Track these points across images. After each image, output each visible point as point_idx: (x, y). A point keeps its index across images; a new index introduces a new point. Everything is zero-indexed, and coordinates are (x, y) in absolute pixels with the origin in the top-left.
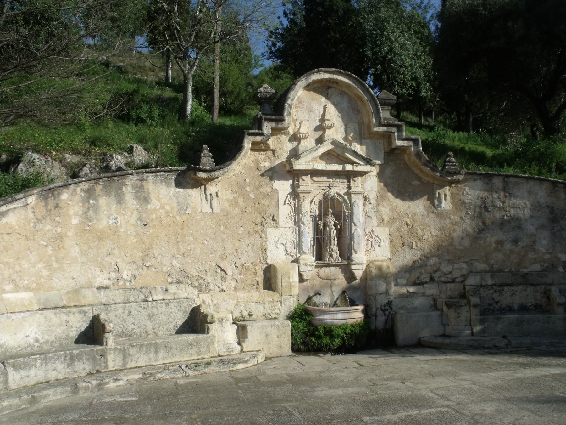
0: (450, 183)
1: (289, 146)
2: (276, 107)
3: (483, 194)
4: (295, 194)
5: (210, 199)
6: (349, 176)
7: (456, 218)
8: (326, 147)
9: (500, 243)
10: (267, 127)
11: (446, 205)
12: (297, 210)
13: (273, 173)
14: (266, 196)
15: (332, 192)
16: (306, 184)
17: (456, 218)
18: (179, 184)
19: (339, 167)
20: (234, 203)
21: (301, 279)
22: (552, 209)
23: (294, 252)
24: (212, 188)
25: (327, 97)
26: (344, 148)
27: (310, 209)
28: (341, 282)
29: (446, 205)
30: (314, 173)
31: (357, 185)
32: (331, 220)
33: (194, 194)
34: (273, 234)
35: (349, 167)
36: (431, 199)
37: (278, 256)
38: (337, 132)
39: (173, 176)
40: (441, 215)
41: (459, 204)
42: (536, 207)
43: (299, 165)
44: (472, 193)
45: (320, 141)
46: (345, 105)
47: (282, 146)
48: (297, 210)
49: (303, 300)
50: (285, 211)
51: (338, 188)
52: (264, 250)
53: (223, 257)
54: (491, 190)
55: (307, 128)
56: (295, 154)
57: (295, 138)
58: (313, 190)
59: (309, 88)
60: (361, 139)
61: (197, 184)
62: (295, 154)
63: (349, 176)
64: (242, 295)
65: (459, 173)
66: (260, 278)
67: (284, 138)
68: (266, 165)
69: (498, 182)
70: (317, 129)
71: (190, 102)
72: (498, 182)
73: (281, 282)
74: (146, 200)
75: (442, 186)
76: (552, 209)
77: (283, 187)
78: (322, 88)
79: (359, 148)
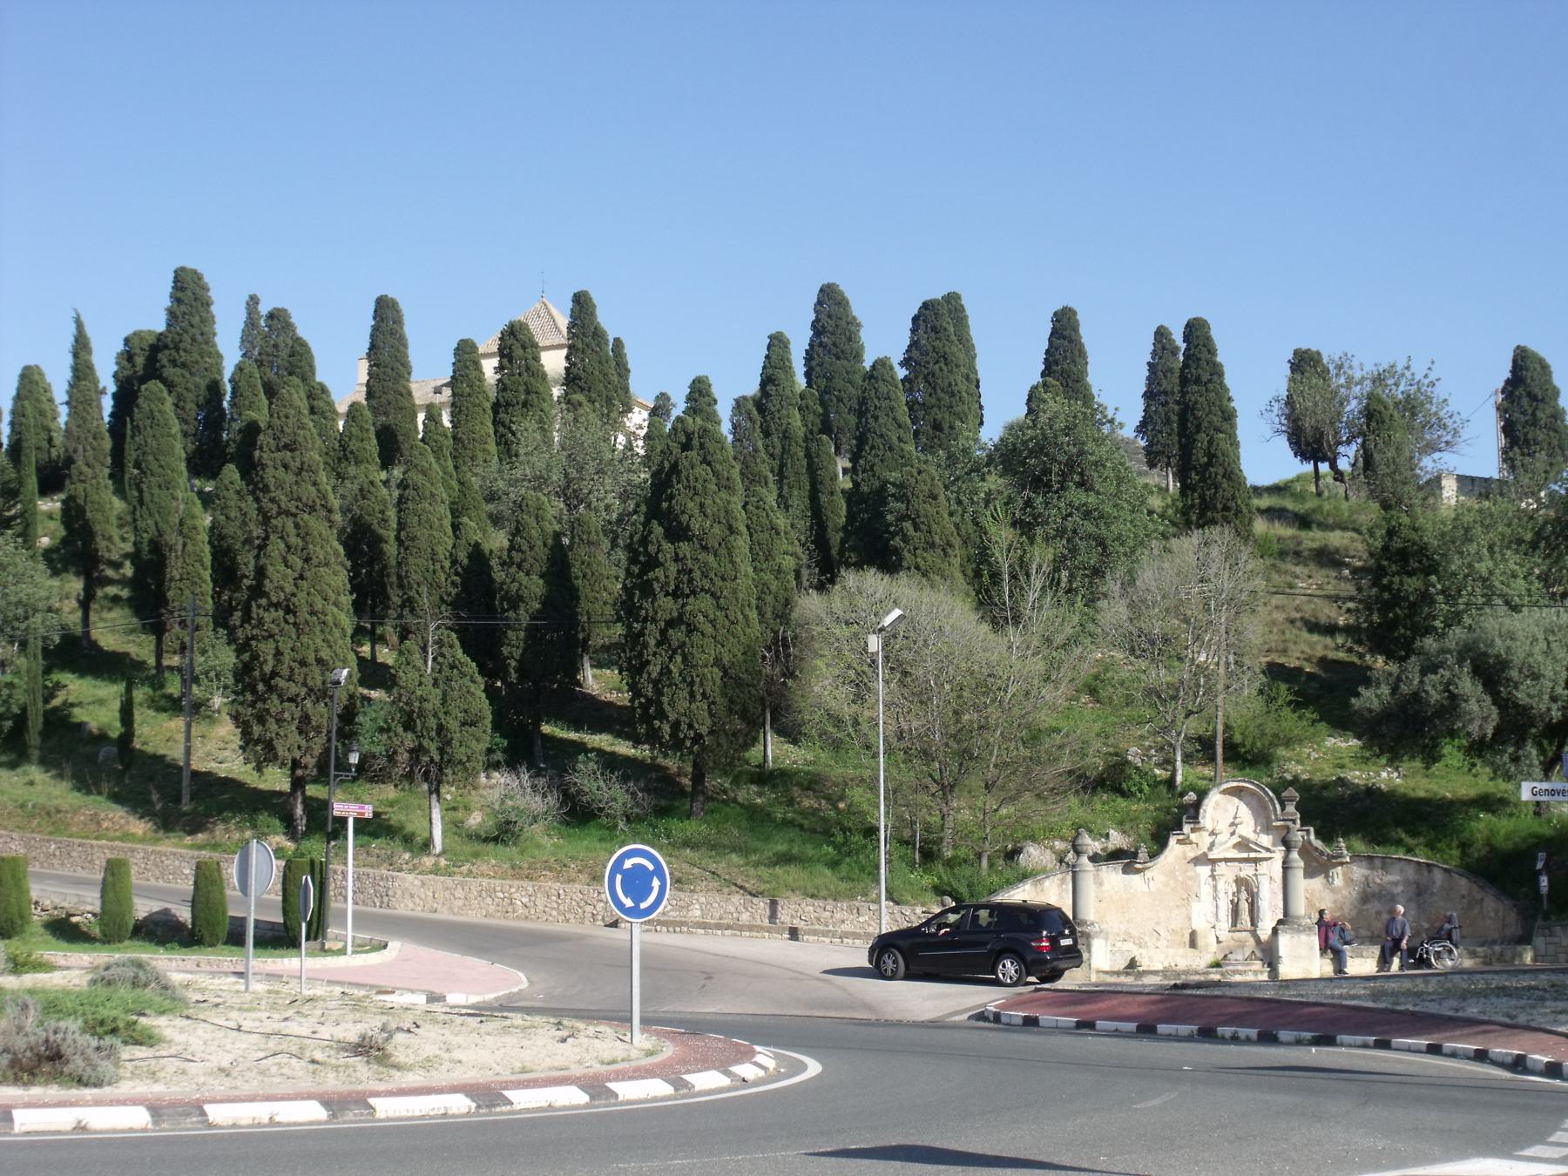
0: (1342, 864)
1: (1210, 839)
2: (1193, 811)
3: (1366, 872)
4: (1213, 877)
5: (1147, 882)
6: (1256, 861)
7: (1345, 893)
8: (1236, 839)
9: (1378, 913)
10: (1187, 828)
11: (1338, 881)
12: (1215, 887)
13: (1197, 861)
14: (1191, 878)
15: (1242, 875)
16: (1221, 868)
17: (1345, 893)
18: (1125, 871)
19: (1245, 855)
20: (1166, 884)
21: (1219, 942)
22: (1418, 884)
23: (1213, 920)
24: (1148, 874)
25: (1240, 798)
26: (1248, 840)
27: (1227, 887)
28: (1251, 941)
29: (1338, 881)
30: (1227, 860)
31: (1263, 867)
32: (1244, 895)
33: (1136, 878)
34: (1196, 907)
35: (1253, 855)
36: (1327, 877)
37: (1199, 924)
38: (1248, 827)
39: (1120, 867)
40: (1334, 891)
41: (1349, 881)
42: (1407, 883)
43: (1211, 856)
44: (1359, 872)
45: (1233, 834)
46: (1254, 803)
47: (1202, 840)
48: (1215, 887)
49: (1220, 957)
50: (1206, 890)
51: (1247, 871)
52: (1190, 919)
53: (1158, 924)
54: (1372, 868)
55: (1223, 827)
56: (1210, 849)
57: (1213, 833)
58: (1227, 873)
59: (1224, 792)
60: (1267, 829)
61: (1138, 871)
62: (1212, 845)
63: (1256, 861)
64: (1171, 951)
65: (1341, 856)
66: (1187, 938)
67: (1205, 834)
68: (1192, 855)
69: (1378, 862)
70: (1233, 824)
71: (1180, 772)
72: (1378, 862)
73: (1200, 942)
74: (1101, 884)
75: (1335, 866)
76: (1418, 884)
77: (1205, 870)
78: (1237, 792)
79: (1266, 840)
